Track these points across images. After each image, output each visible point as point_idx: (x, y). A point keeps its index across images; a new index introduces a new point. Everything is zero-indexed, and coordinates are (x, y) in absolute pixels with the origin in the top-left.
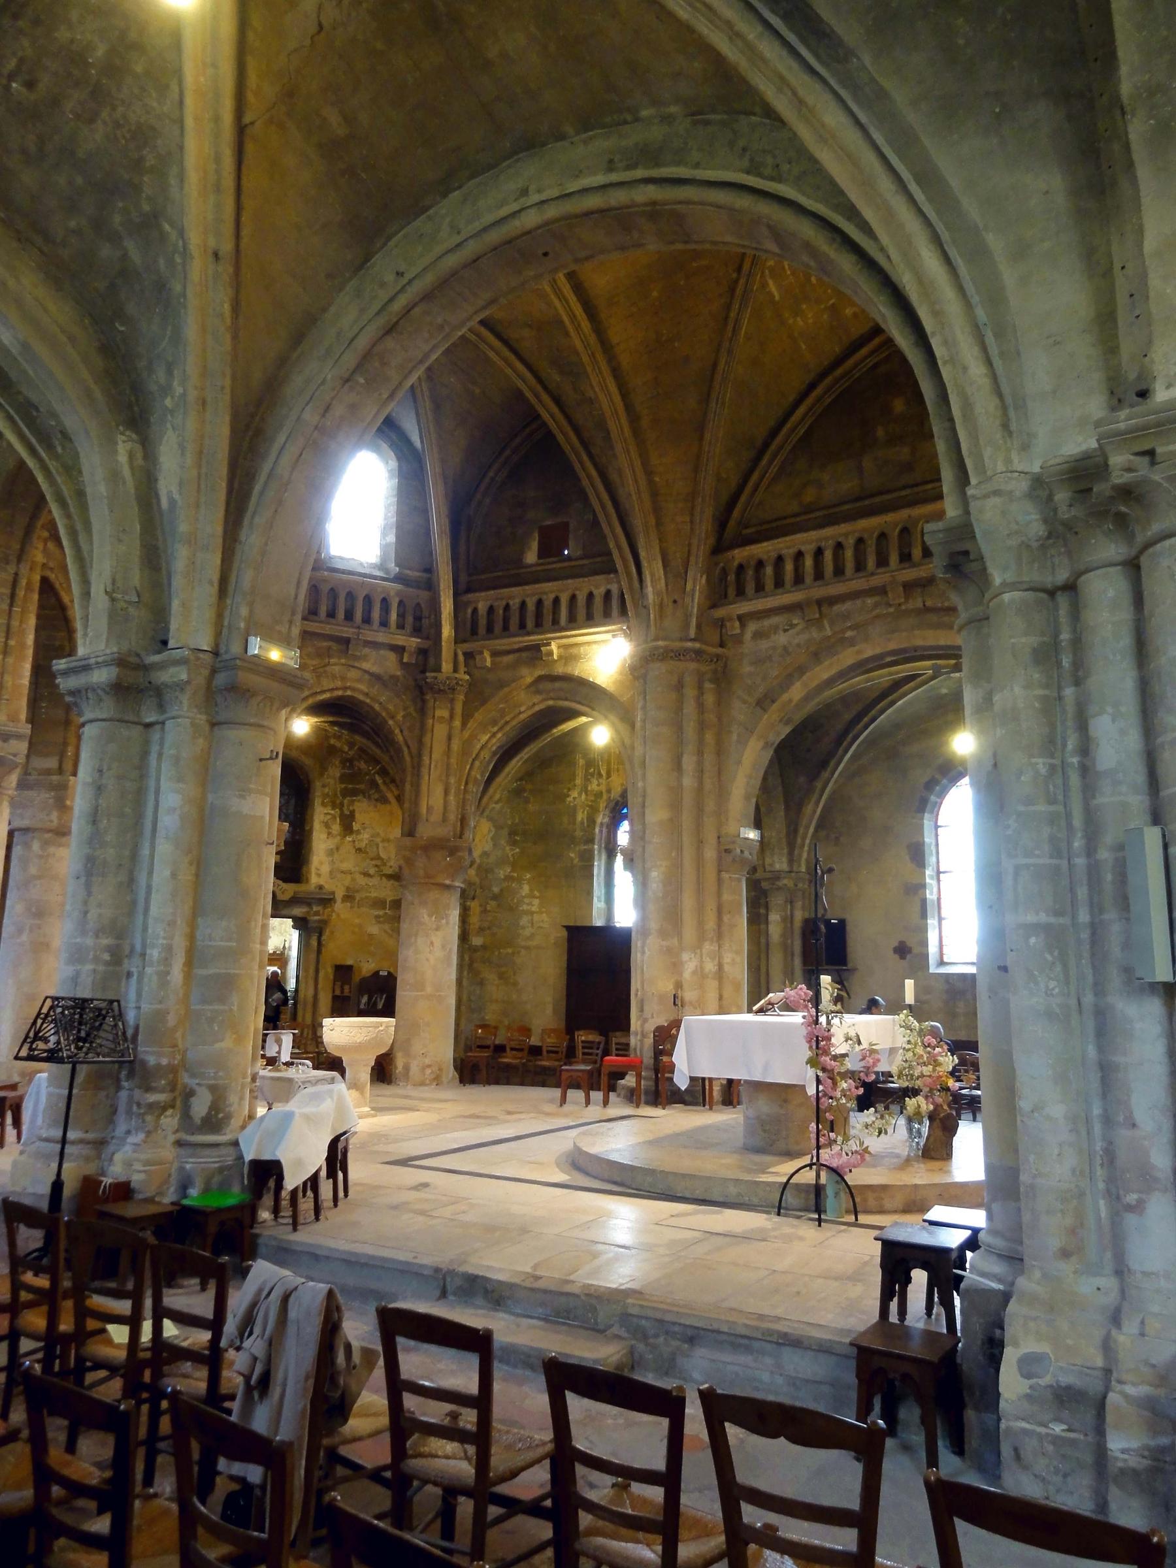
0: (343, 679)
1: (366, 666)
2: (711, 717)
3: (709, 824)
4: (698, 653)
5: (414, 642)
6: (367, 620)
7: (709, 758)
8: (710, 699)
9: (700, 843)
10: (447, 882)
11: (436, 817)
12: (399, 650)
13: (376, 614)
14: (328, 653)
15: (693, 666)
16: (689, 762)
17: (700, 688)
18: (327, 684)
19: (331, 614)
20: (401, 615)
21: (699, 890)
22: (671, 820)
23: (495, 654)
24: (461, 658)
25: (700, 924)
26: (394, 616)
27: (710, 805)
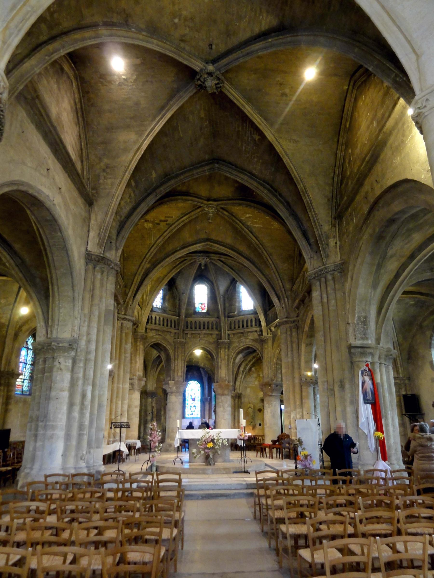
0: (246, 342)
1: (250, 338)
2: (295, 340)
3: (296, 371)
4: (286, 321)
5: (258, 329)
6: (247, 326)
7: (295, 352)
8: (294, 334)
9: (294, 378)
10: (270, 394)
11: (266, 376)
12: (256, 331)
13: (249, 324)
14: (240, 337)
15: (287, 325)
16: (290, 353)
17: (291, 330)
18: (242, 345)
19: (239, 327)
20: (256, 322)
21: (294, 392)
22: (286, 372)
23: (275, 327)
24: (269, 330)
25: (295, 403)
26: (254, 323)
27: (296, 366)
